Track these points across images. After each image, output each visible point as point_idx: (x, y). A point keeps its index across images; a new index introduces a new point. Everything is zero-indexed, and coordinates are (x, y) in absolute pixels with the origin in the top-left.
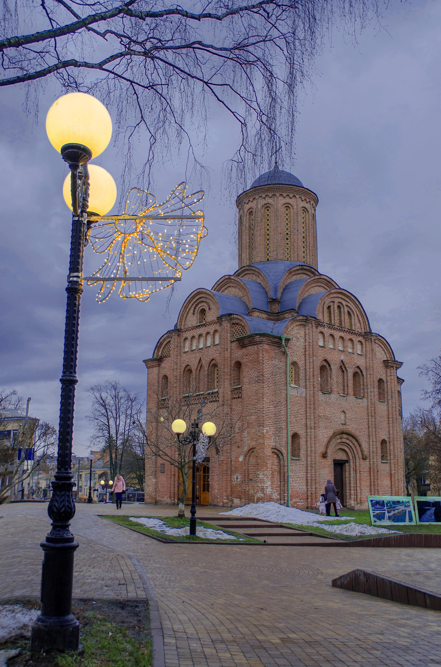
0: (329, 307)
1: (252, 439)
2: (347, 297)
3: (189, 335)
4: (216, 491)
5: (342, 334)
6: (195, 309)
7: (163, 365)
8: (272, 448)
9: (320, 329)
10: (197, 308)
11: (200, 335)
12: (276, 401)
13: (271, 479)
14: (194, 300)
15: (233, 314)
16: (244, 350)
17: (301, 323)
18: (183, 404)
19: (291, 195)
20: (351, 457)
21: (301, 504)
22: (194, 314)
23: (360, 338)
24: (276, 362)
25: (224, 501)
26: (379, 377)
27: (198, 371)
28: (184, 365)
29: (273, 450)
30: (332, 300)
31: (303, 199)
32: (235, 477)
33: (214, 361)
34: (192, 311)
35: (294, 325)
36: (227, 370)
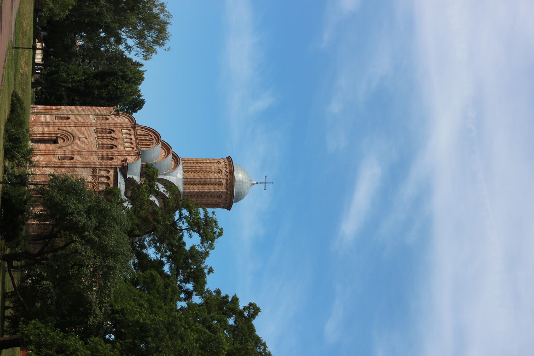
5: (134, 139)
26: (114, 157)
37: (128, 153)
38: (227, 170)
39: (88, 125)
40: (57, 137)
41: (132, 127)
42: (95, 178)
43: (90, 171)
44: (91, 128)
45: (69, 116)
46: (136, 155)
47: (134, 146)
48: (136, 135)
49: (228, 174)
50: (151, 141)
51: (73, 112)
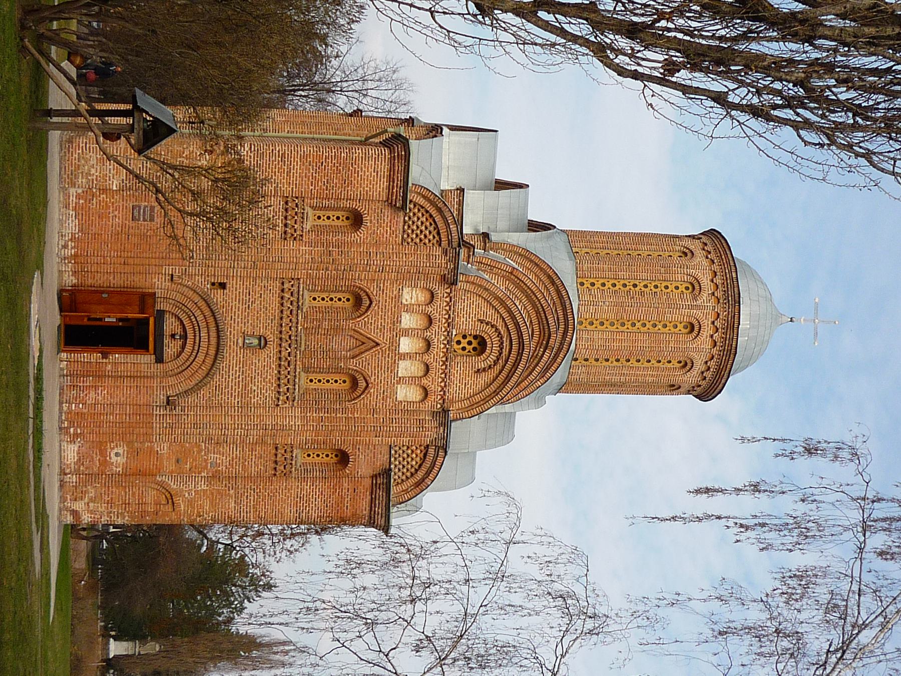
1: (190, 503)
3: (438, 310)
4: (92, 394)
6: (492, 326)
7: (387, 212)
10: (491, 331)
11: (428, 345)
14: (511, 326)
15: (446, 454)
16: (367, 482)
18: (286, 286)
22: (482, 321)
25: (72, 430)
27: (352, 333)
28: (373, 290)
32: (121, 451)
33: (364, 384)
34: (491, 315)
36: (337, 439)
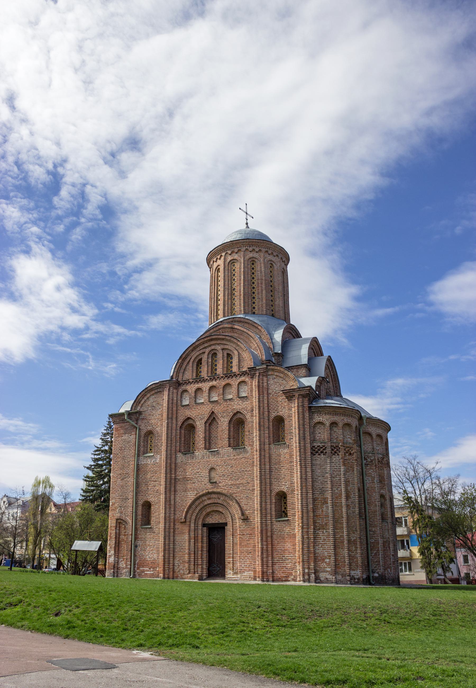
0: (201, 360)
2: (223, 339)
5: (214, 383)
8: (117, 520)
9: (184, 387)
12: (123, 474)
13: (115, 548)
17: (156, 391)
19: (219, 257)
20: (229, 520)
21: (149, 572)
23: (243, 378)
24: (125, 437)
26: (273, 415)
29: (119, 521)
30: (201, 352)
31: (229, 252)
35: (148, 395)
37: (263, 391)
38: (251, 249)
39: (172, 467)
40: (204, 525)
41: (177, 389)
42: (335, 450)
43: (320, 459)
44: (179, 461)
45: (140, 503)
46: (267, 376)
47: (234, 382)
48: (198, 379)
49: (257, 249)
50: (215, 355)
51: (131, 495)
